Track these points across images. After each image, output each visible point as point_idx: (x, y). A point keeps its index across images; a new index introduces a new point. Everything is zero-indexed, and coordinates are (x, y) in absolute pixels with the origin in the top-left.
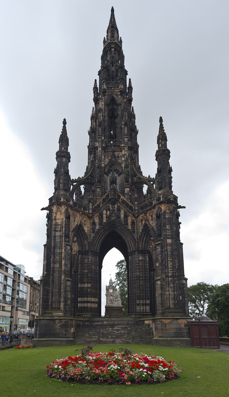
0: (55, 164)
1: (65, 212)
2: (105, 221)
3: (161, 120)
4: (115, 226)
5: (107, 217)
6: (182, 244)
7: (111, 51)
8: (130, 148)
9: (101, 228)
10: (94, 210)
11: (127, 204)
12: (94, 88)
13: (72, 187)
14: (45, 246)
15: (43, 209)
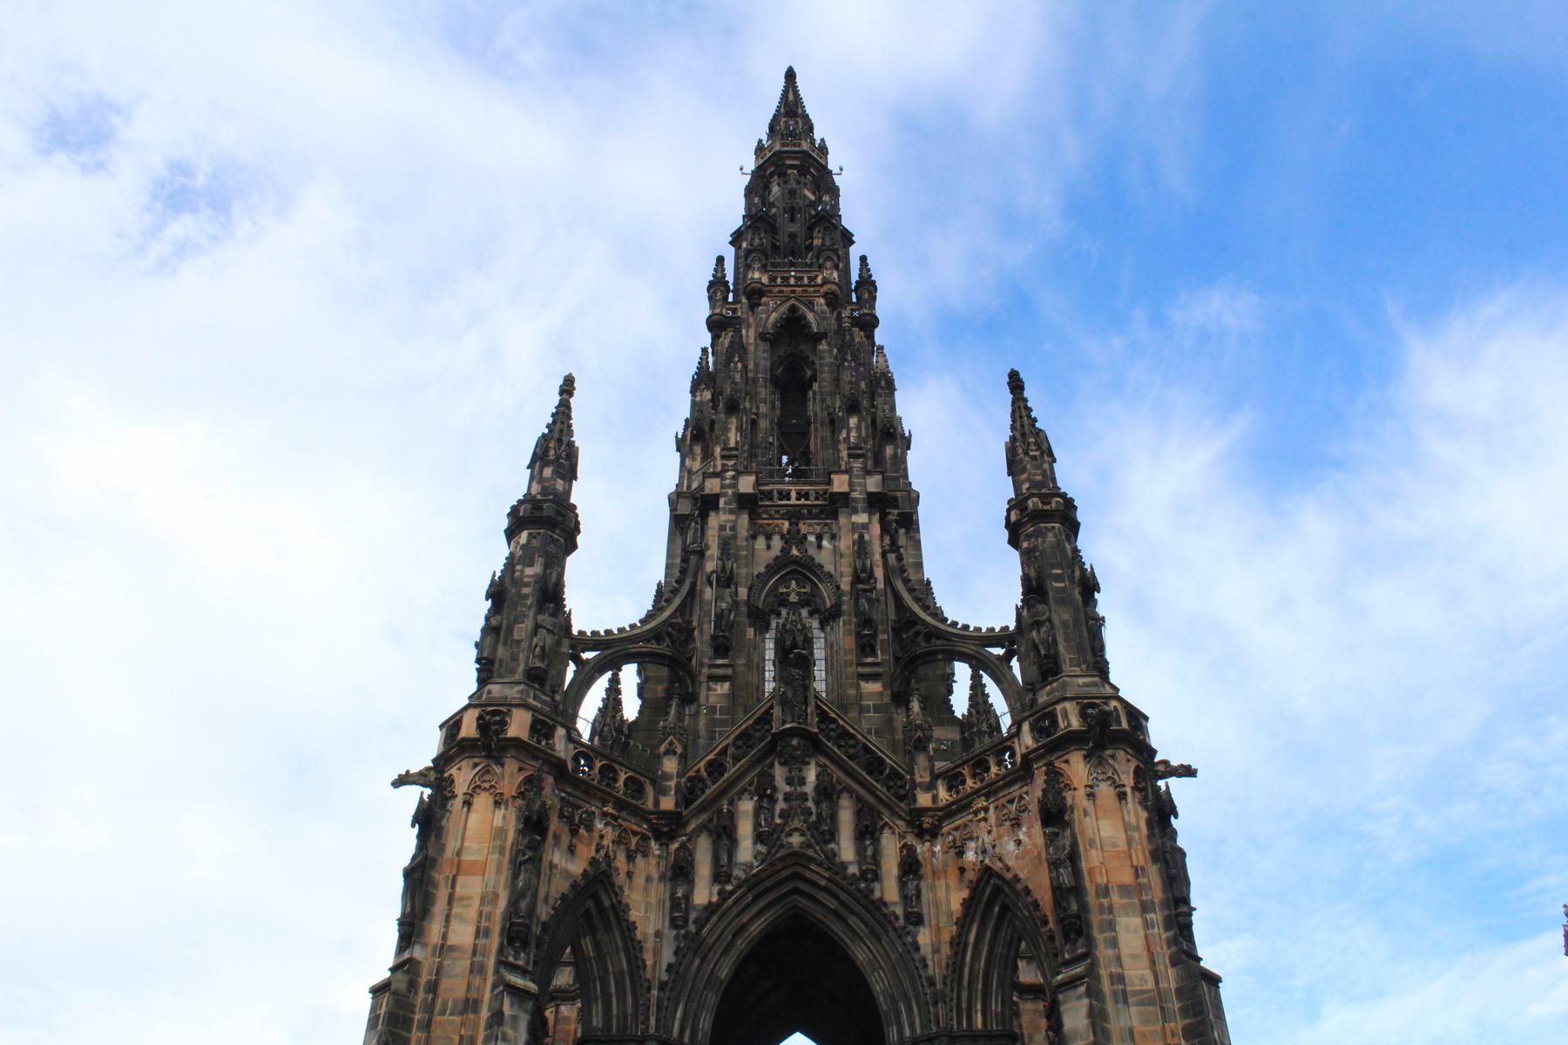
0: (494, 555)
1: (521, 795)
2: (746, 850)
3: (1016, 383)
4: (803, 886)
5: (759, 838)
6: (1213, 980)
7: (782, 175)
8: (877, 503)
9: (720, 893)
10: (687, 796)
11: (875, 764)
12: (711, 285)
13: (572, 667)
14: (377, 991)
15: (401, 781)
